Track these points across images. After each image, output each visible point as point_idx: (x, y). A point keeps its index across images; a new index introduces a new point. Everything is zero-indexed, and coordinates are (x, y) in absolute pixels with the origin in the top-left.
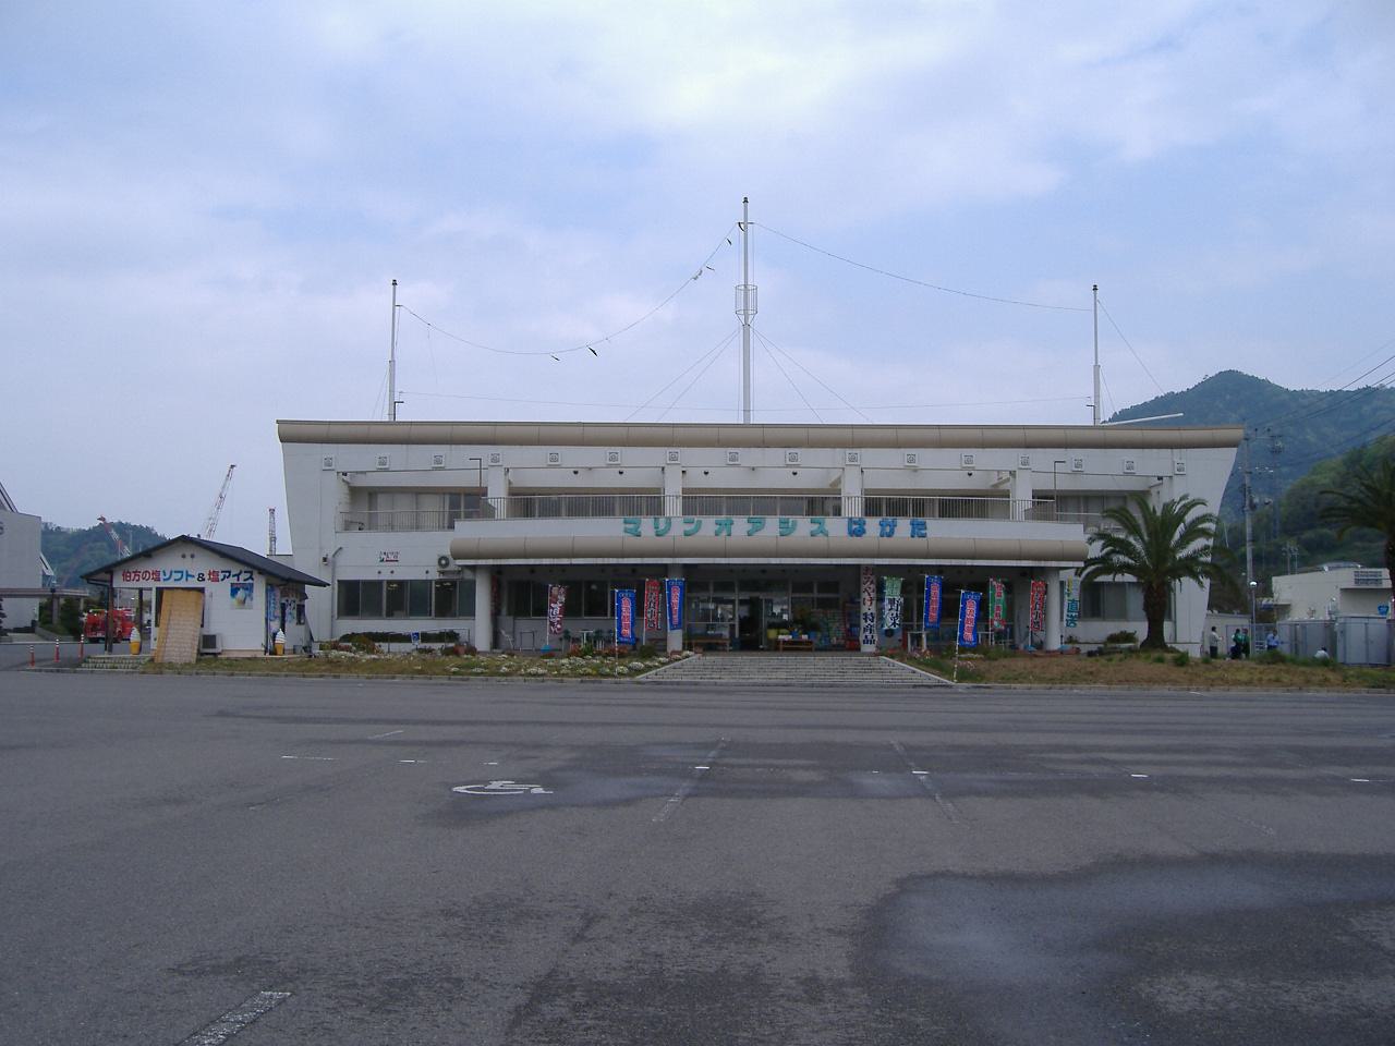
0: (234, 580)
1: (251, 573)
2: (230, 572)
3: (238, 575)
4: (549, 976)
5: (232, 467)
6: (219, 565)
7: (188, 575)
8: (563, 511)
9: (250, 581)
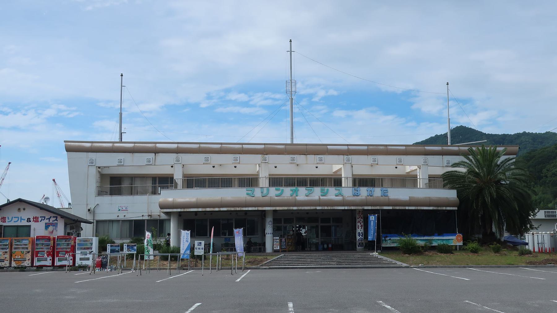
0: (47, 221)
1: (57, 217)
2: (45, 217)
3: (49, 219)
4: (521, 255)
5: (9, 163)
6: (38, 213)
7: (21, 219)
8: (296, 184)
9: (56, 222)
